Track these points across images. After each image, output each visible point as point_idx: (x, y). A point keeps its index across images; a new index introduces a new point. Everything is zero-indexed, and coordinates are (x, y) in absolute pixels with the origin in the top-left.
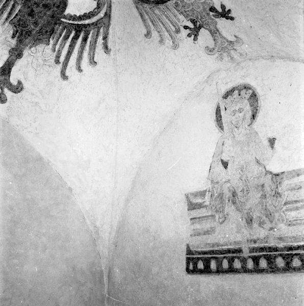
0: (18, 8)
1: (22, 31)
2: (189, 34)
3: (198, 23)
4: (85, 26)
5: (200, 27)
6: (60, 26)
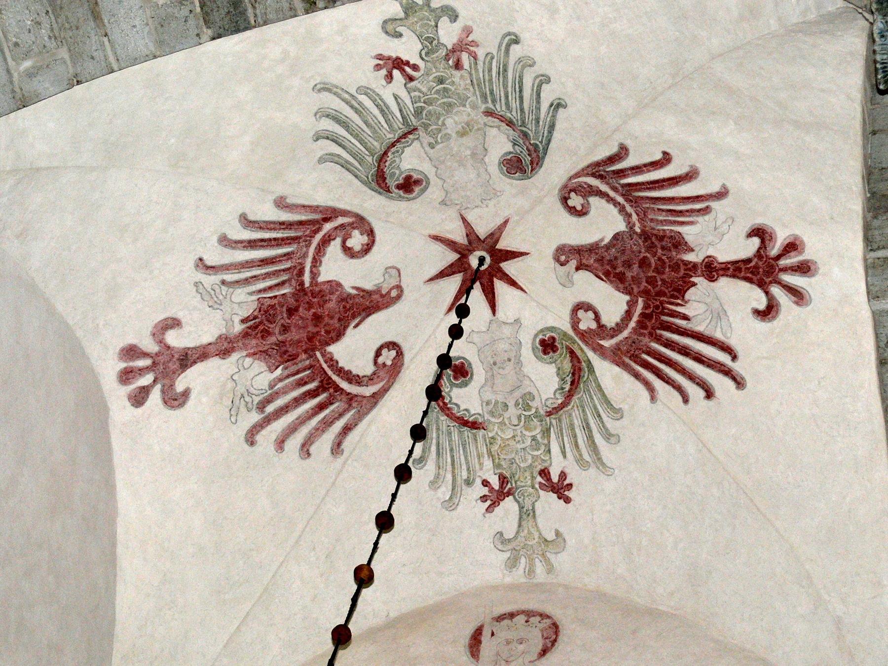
0: (286, 290)
1: (261, 323)
2: (485, 496)
3: (509, 486)
4: (338, 389)
5: (509, 494)
6: (308, 359)
